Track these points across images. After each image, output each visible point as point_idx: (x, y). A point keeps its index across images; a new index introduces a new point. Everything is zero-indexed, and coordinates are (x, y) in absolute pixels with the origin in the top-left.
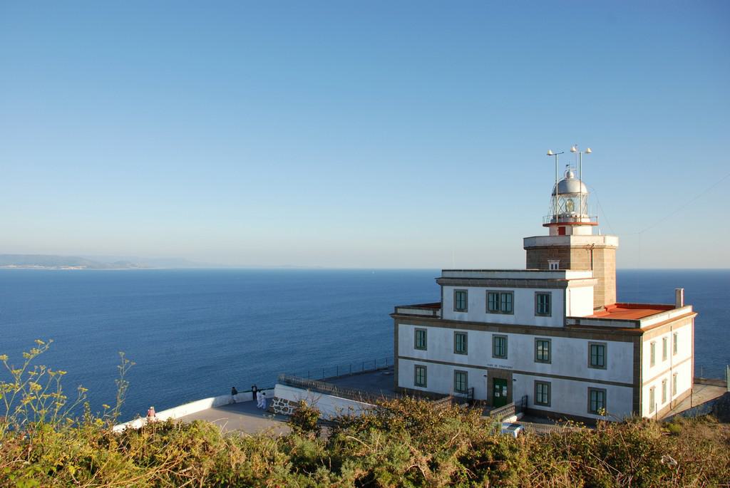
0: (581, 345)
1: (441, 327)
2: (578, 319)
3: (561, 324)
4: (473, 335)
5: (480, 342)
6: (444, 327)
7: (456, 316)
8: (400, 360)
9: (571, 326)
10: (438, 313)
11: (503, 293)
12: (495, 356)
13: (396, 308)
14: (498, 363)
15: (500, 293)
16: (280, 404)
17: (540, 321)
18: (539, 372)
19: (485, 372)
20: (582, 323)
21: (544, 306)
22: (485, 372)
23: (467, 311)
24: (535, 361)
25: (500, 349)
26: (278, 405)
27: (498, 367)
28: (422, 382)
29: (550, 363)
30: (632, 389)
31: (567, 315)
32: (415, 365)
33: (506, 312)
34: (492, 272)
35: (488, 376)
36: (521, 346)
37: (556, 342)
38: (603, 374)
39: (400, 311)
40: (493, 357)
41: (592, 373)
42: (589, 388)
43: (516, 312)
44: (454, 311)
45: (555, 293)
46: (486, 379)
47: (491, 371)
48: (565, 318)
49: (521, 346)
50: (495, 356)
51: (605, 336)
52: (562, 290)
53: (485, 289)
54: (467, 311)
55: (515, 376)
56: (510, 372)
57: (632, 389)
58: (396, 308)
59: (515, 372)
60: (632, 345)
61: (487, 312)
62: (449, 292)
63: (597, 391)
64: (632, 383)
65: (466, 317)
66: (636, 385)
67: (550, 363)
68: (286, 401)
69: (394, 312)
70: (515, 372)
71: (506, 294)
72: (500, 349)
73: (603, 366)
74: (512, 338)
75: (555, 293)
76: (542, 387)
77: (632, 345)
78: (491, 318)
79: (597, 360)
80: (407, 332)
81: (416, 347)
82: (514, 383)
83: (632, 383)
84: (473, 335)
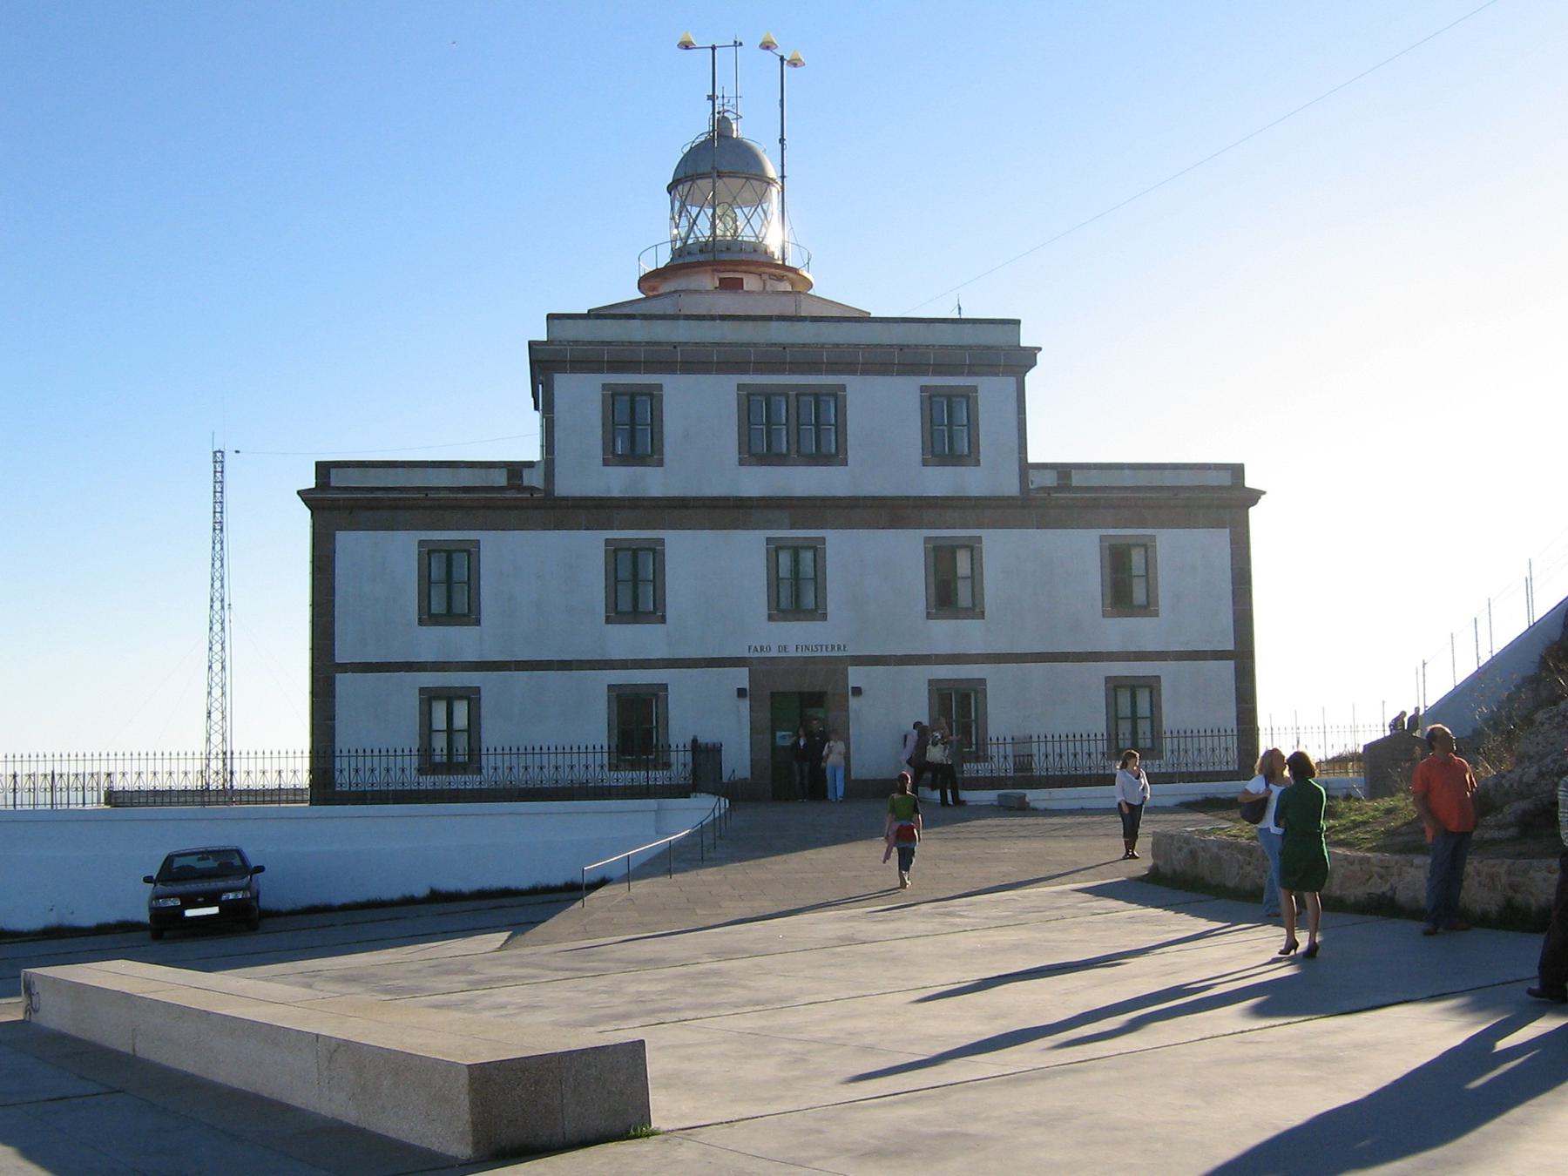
1: (546, 527)
2: (1064, 470)
3: (1011, 487)
4: (687, 554)
5: (719, 580)
6: (557, 527)
7: (618, 482)
8: (343, 682)
10: (533, 479)
11: (801, 392)
13: (323, 468)
14: (793, 639)
15: (792, 393)
17: (940, 482)
19: (742, 677)
20: (1077, 479)
21: (949, 432)
22: (742, 677)
23: (660, 463)
24: (929, 616)
27: (792, 653)
29: (982, 615)
30: (1231, 664)
32: (422, 690)
34: (736, 324)
39: (337, 479)
40: (770, 618)
41: (1119, 633)
42: (1108, 679)
44: (606, 463)
48: (1025, 467)
49: (873, 577)
52: (1012, 380)
53: (734, 380)
54: (660, 463)
56: (837, 665)
57: (1231, 664)
58: (323, 468)
60: (1222, 537)
62: (582, 393)
63: (1133, 685)
65: (653, 482)
66: (1242, 657)
67: (982, 615)
69: (310, 483)
71: (818, 395)
75: (990, 390)
76: (958, 706)
77: (1222, 537)
79: (1124, 588)
80: (389, 558)
81: (428, 617)
82: (854, 703)
83: (1230, 646)
84: (687, 554)
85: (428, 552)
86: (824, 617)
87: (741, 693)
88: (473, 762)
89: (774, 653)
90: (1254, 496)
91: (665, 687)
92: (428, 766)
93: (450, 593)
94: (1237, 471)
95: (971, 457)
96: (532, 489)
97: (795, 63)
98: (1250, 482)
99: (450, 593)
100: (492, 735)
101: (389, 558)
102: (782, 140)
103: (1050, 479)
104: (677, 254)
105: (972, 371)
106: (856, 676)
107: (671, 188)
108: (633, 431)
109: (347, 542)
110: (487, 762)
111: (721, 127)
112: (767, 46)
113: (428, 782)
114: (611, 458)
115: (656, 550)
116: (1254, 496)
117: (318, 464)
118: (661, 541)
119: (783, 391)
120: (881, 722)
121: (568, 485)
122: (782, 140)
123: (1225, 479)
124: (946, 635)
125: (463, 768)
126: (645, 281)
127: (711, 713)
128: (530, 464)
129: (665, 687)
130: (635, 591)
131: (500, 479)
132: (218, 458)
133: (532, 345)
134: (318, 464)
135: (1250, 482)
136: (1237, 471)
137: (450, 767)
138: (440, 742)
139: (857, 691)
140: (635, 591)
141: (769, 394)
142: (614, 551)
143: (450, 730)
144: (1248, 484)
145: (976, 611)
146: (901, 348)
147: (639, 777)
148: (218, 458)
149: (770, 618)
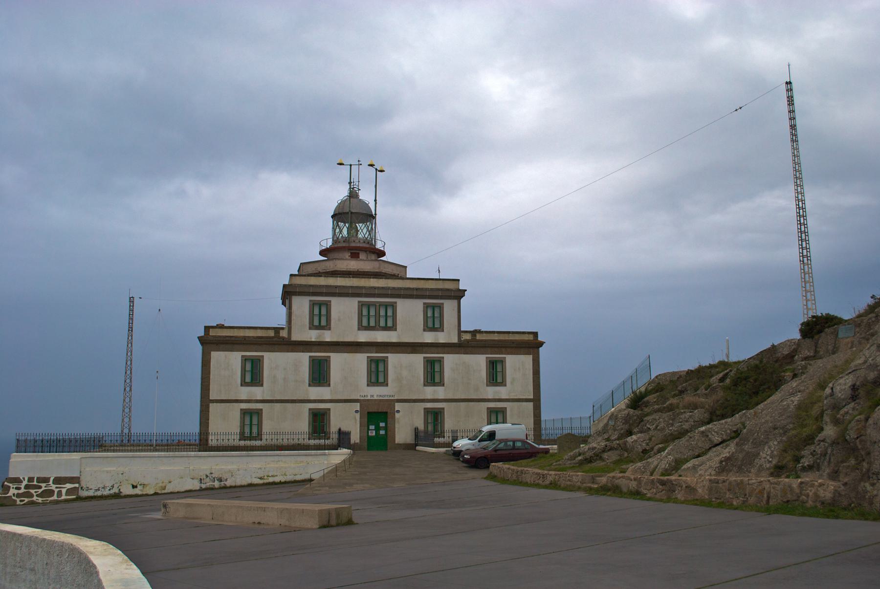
0: (479, 362)
2: (474, 333)
3: (455, 340)
4: (337, 360)
7: (313, 336)
8: (213, 407)
9: (468, 341)
10: (284, 334)
11: (381, 304)
12: (370, 383)
13: (207, 329)
14: (376, 393)
16: (27, 487)
17: (429, 338)
18: (429, 397)
19: (357, 406)
20: (479, 337)
22: (357, 406)
23: (330, 329)
25: (377, 374)
26: (22, 490)
28: (255, 434)
29: (443, 385)
30: (531, 404)
31: (462, 329)
33: (386, 328)
35: (361, 412)
36: (405, 369)
37: (450, 360)
38: (502, 392)
39: (212, 333)
40: (368, 385)
43: (399, 327)
45: (449, 306)
46: (358, 416)
47: (364, 403)
50: (370, 383)
51: (503, 350)
52: (456, 301)
54: (330, 329)
55: (398, 406)
56: (391, 402)
57: (531, 404)
58: (207, 329)
59: (399, 401)
61: (359, 329)
62: (302, 305)
64: (532, 397)
65: (328, 336)
66: (536, 401)
67: (443, 385)
68: (46, 480)
70: (399, 401)
71: (386, 306)
72: (377, 374)
73: (503, 383)
74: (393, 359)
75: (449, 306)
78: (364, 337)
79: (495, 374)
80: (228, 364)
81: (244, 383)
82: (397, 415)
83: (532, 397)
84: (337, 360)
85: (245, 359)
86: (387, 385)
87: (357, 411)
88: (259, 437)
89: (369, 398)
90: (541, 344)
91: (329, 409)
92: (243, 437)
93: (253, 374)
94: (535, 334)
95: (441, 329)
96: (283, 338)
97: (382, 171)
98: (540, 339)
99: (253, 374)
100: (267, 427)
101: (228, 364)
102: (375, 200)
103: (468, 337)
104: (335, 240)
105: (442, 297)
106: (398, 406)
107: (332, 217)
108: (321, 318)
109: (217, 356)
110: (264, 437)
111: (353, 194)
112: (372, 165)
113: (242, 443)
114: (312, 327)
115: (327, 360)
116: (541, 344)
117: (206, 327)
118: (329, 357)
119: (374, 304)
120: (406, 424)
121: (296, 337)
122: (375, 200)
123: (531, 337)
124: (430, 392)
125: (255, 439)
126: (323, 253)
127: (346, 420)
128: (283, 328)
129: (329, 409)
130: (319, 374)
131: (271, 333)
132: (132, 300)
133: (284, 286)
134: (206, 327)
135: (540, 339)
136: (535, 334)
137: (251, 438)
138: (247, 430)
139: (398, 411)
140: (319, 374)
141: (369, 305)
142: (313, 360)
143: (251, 425)
144: (540, 339)
145: (441, 383)
146: (417, 289)
147: (317, 442)
148: (132, 300)
149: (368, 385)
